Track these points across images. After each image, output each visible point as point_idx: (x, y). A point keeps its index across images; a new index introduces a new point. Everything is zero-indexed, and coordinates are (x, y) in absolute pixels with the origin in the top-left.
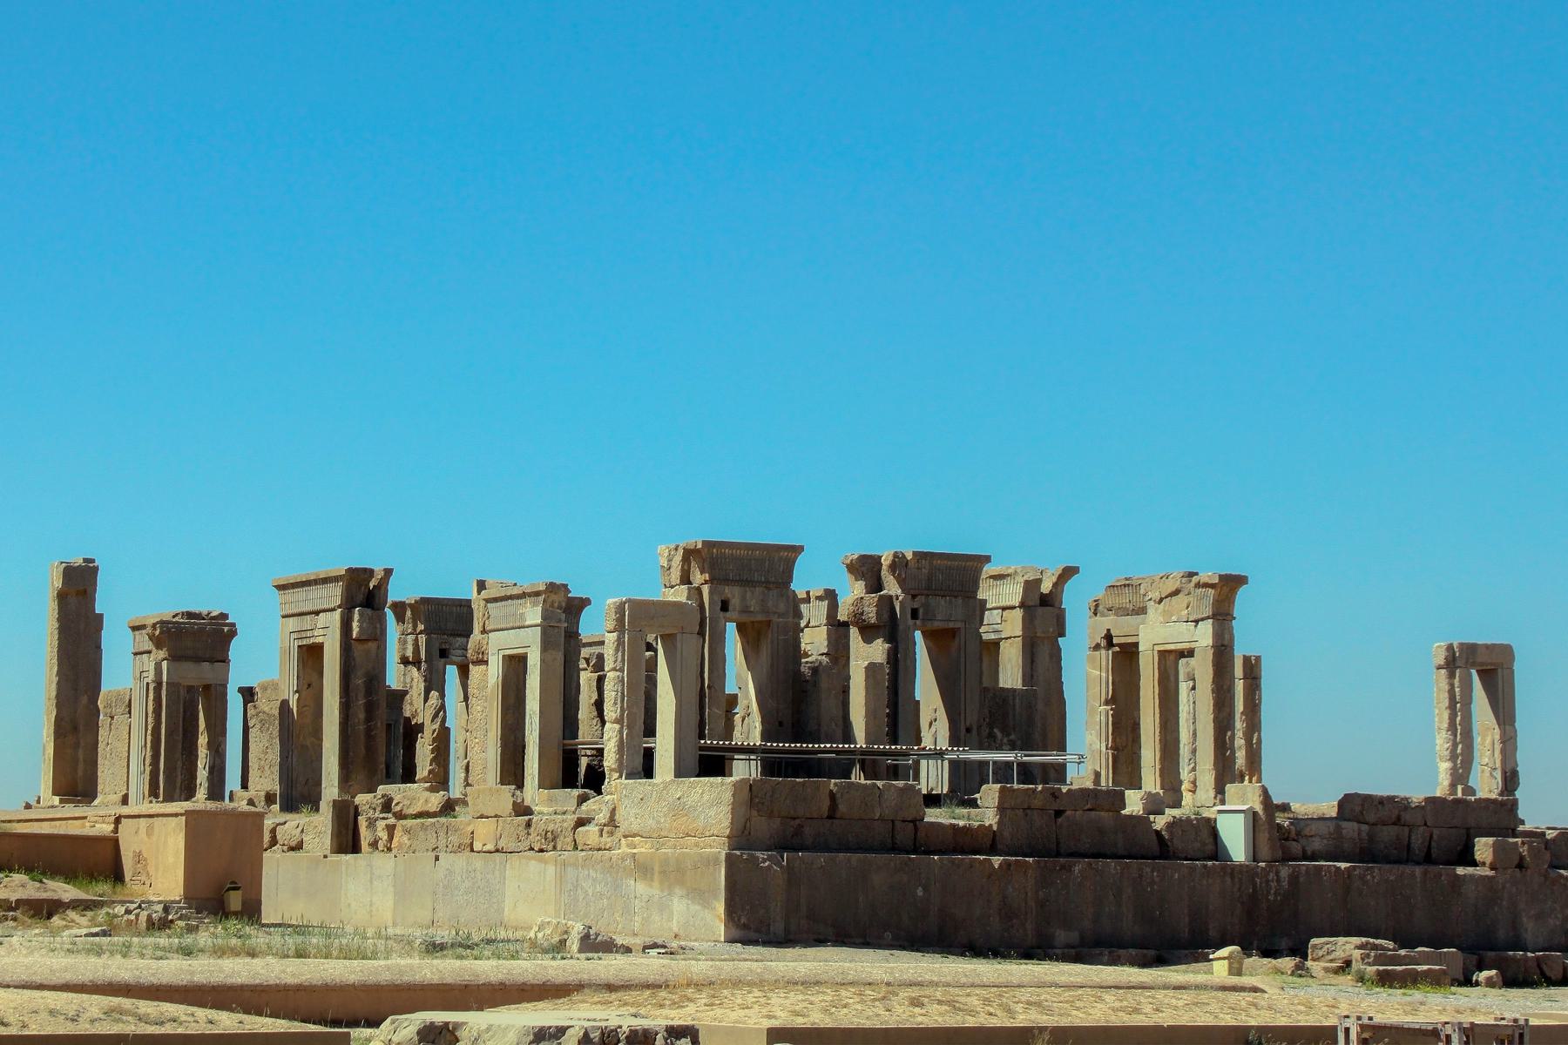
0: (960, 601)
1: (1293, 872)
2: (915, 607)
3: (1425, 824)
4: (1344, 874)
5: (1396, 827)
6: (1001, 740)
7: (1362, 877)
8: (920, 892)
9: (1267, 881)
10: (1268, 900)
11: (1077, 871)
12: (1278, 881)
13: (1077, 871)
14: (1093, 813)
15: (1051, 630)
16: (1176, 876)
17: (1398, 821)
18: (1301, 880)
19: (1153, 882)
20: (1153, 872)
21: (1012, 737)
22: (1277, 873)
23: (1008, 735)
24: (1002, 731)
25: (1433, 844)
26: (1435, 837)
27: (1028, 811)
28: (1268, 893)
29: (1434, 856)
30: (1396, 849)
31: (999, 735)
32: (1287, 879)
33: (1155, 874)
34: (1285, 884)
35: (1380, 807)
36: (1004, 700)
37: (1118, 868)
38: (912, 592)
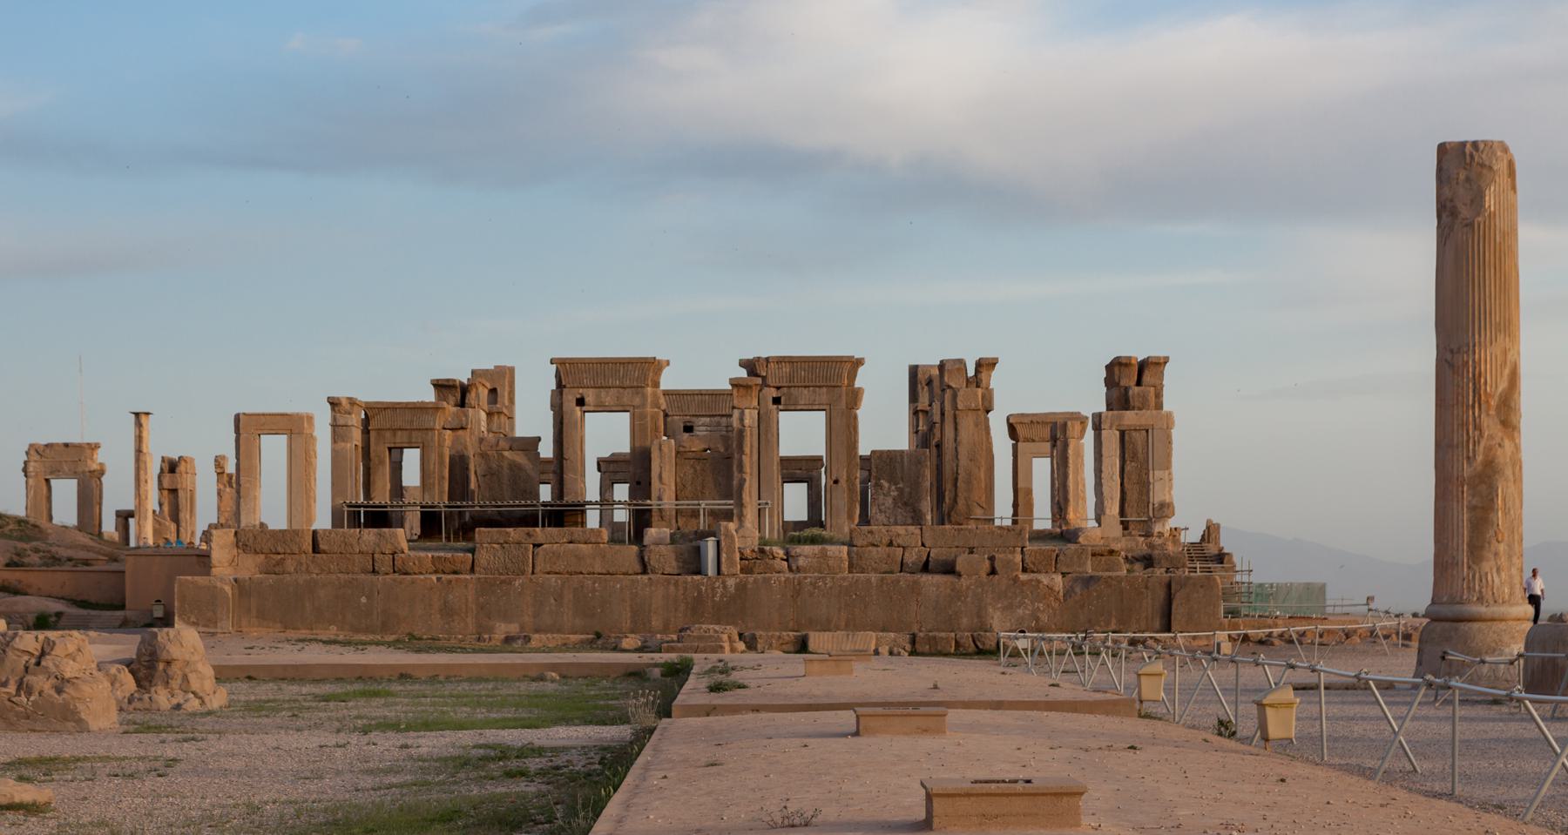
6: (889, 488)
7: (814, 585)
8: (363, 600)
9: (713, 589)
10: (714, 601)
12: (725, 587)
13: (517, 585)
14: (571, 545)
16: (618, 586)
17: (890, 544)
19: (594, 590)
21: (901, 485)
22: (724, 582)
23: (896, 484)
24: (889, 482)
25: (930, 559)
27: (505, 545)
29: (930, 567)
30: (886, 563)
31: (886, 485)
33: (597, 585)
34: (732, 590)
35: (869, 535)
36: (891, 459)
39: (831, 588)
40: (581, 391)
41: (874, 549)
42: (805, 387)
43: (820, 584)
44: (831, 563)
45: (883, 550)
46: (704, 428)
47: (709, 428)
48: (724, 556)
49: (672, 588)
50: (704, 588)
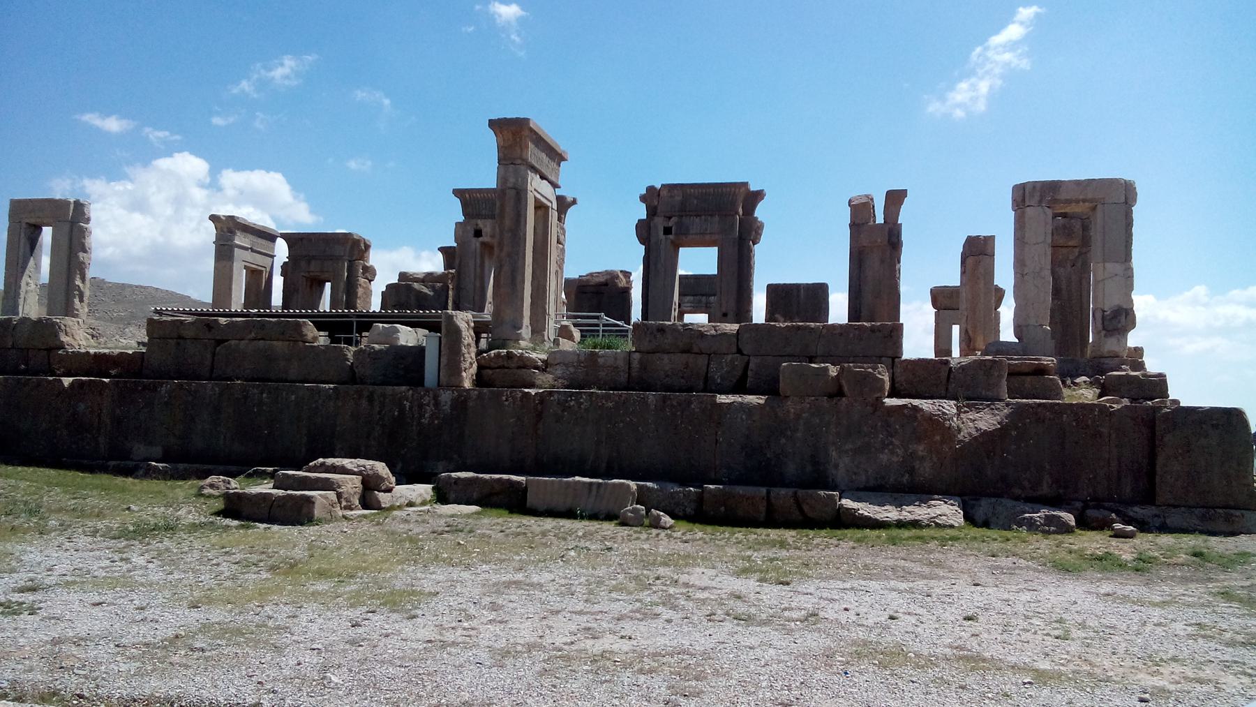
0: (717, 218)
1: (460, 396)
2: (670, 225)
3: (739, 351)
4: (534, 400)
5: (685, 356)
9: (421, 406)
11: (163, 392)
12: (437, 404)
13: (163, 392)
15: (879, 240)
17: (687, 351)
18: (471, 404)
20: (262, 393)
25: (750, 373)
26: (751, 365)
28: (422, 416)
30: (682, 377)
32: (449, 403)
33: (264, 395)
34: (447, 408)
37: (217, 389)
38: (667, 215)
39: (587, 410)
40: (479, 222)
41: (666, 357)
42: (697, 216)
43: (572, 404)
44: (602, 374)
45: (680, 359)
46: (689, 305)
47: (693, 305)
48: (444, 360)
49: (364, 403)
50: (408, 404)
